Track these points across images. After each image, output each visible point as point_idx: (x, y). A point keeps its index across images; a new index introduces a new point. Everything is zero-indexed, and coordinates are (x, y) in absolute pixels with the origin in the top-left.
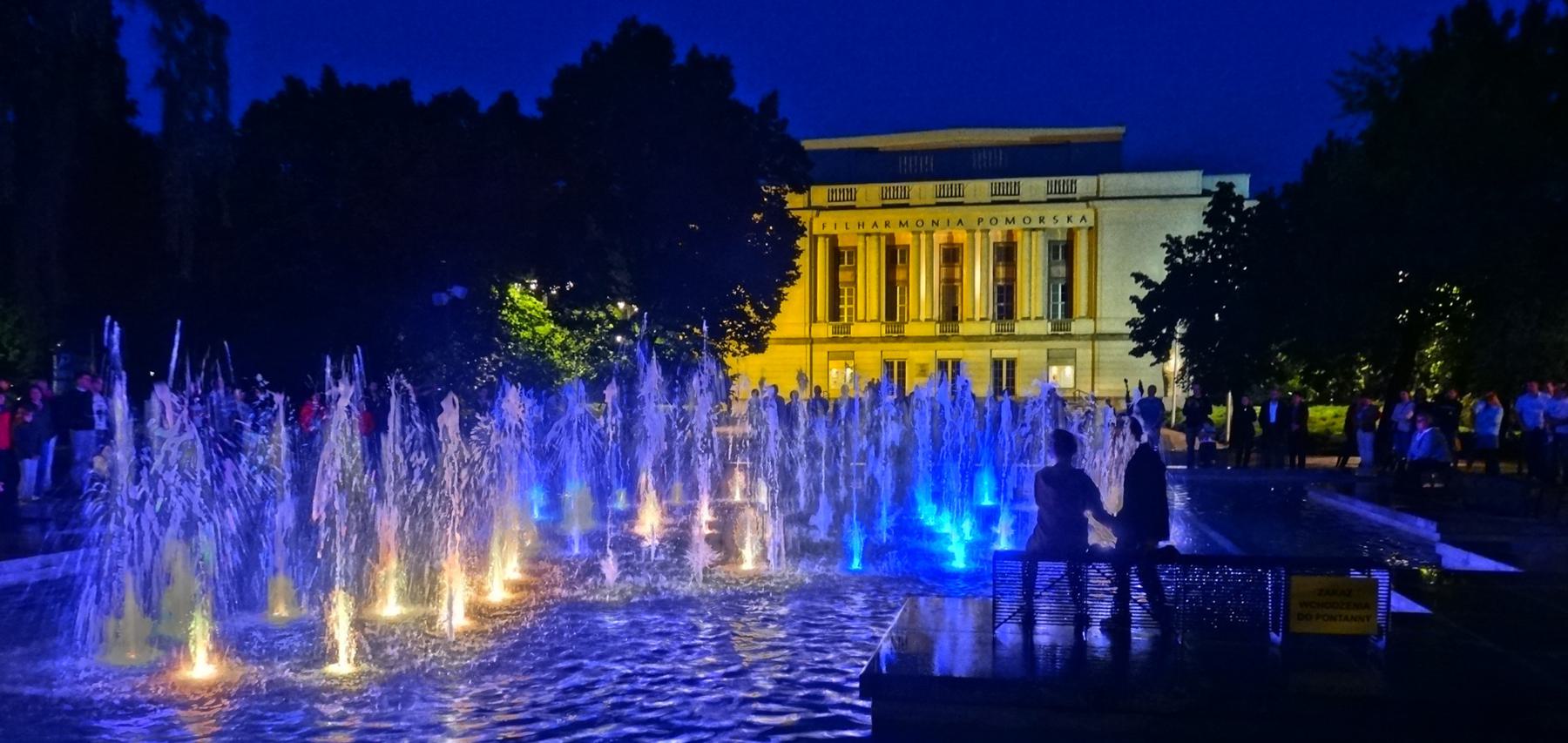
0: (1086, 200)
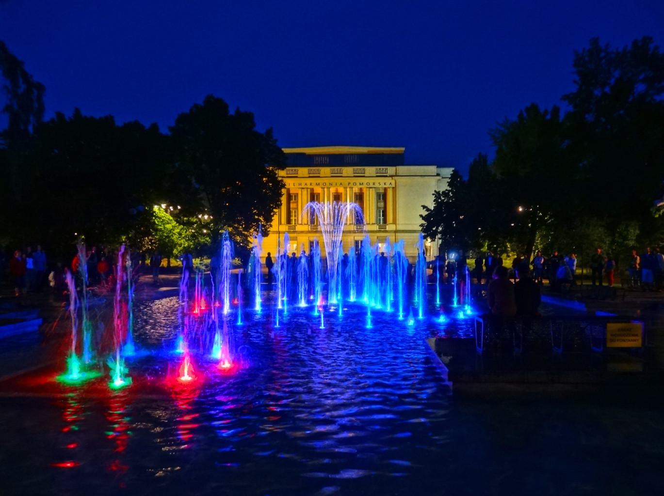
0: (392, 176)
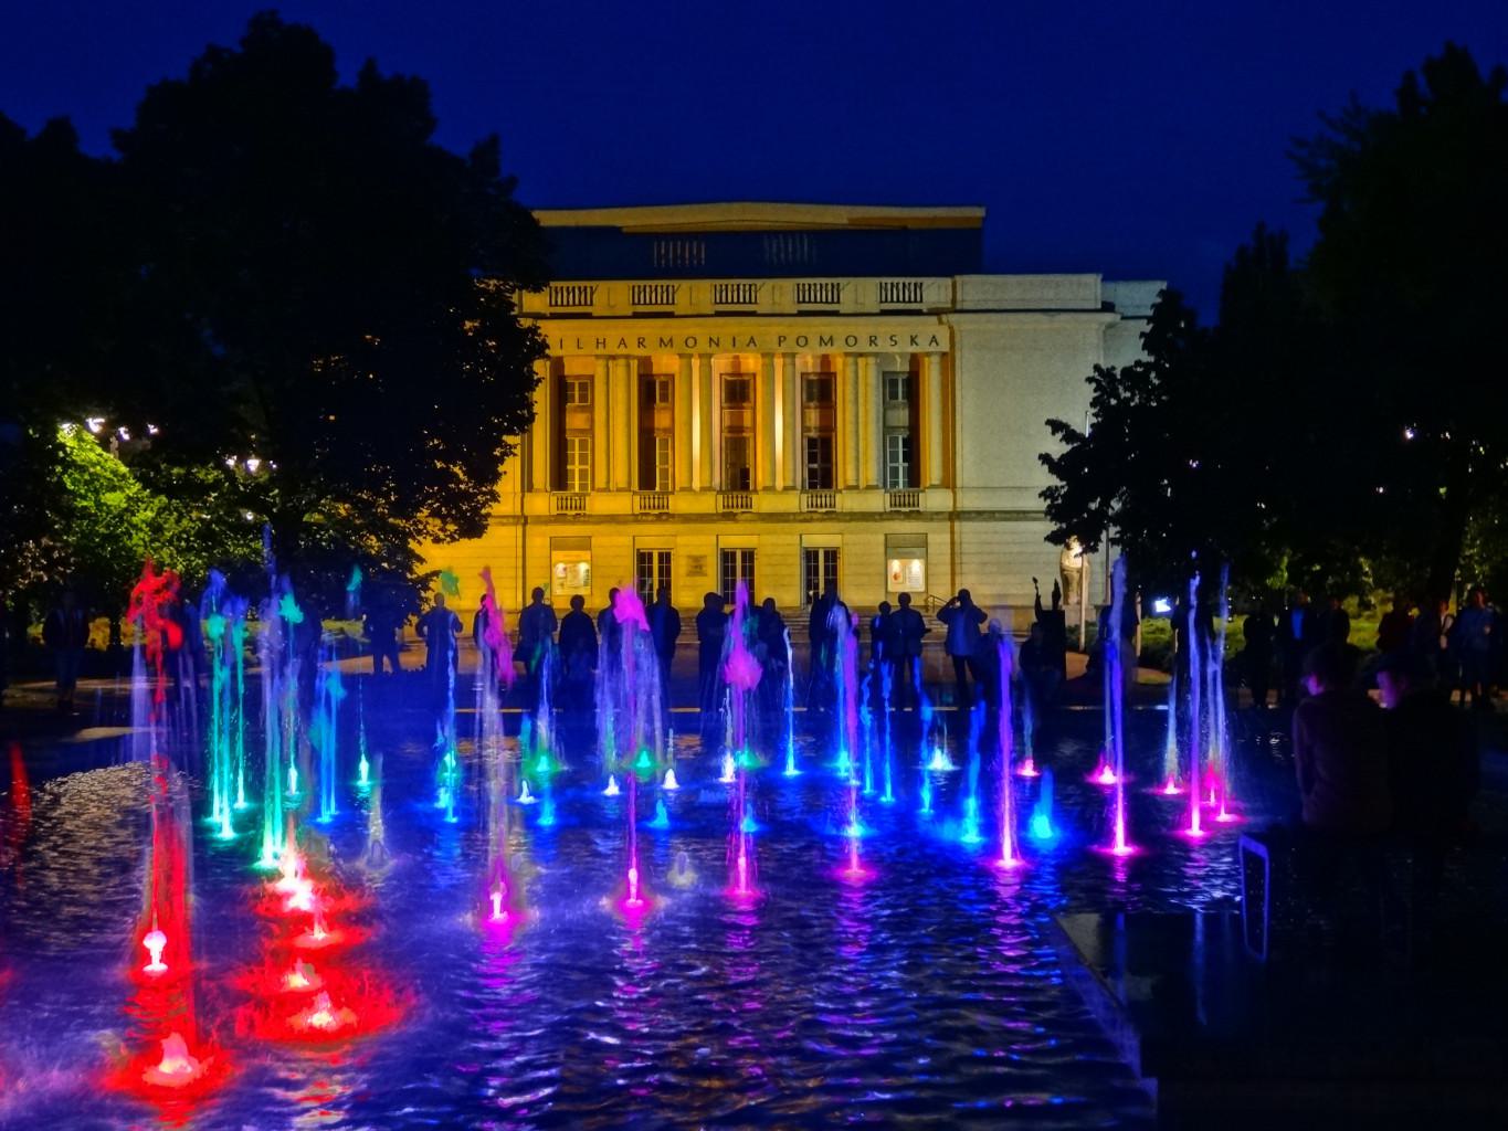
0: (936, 312)
